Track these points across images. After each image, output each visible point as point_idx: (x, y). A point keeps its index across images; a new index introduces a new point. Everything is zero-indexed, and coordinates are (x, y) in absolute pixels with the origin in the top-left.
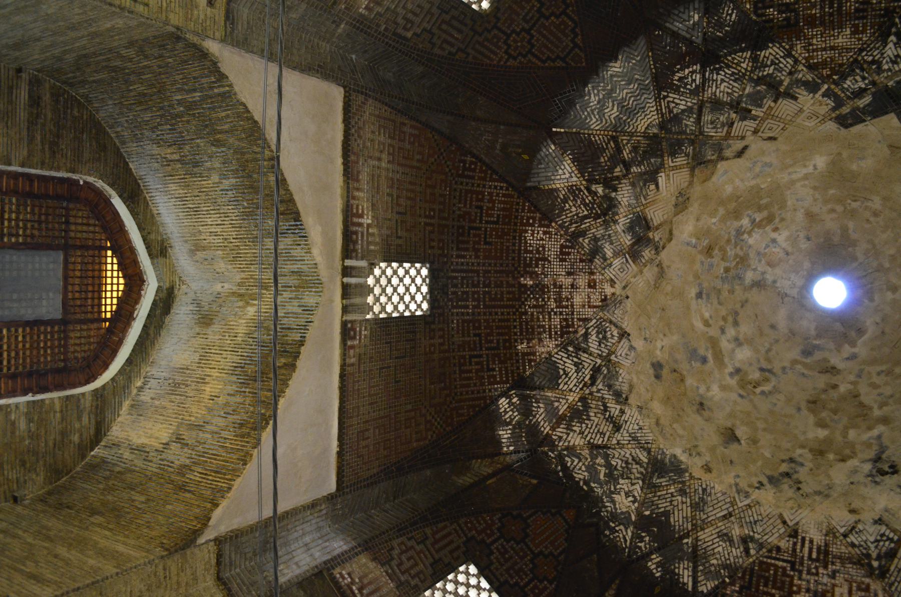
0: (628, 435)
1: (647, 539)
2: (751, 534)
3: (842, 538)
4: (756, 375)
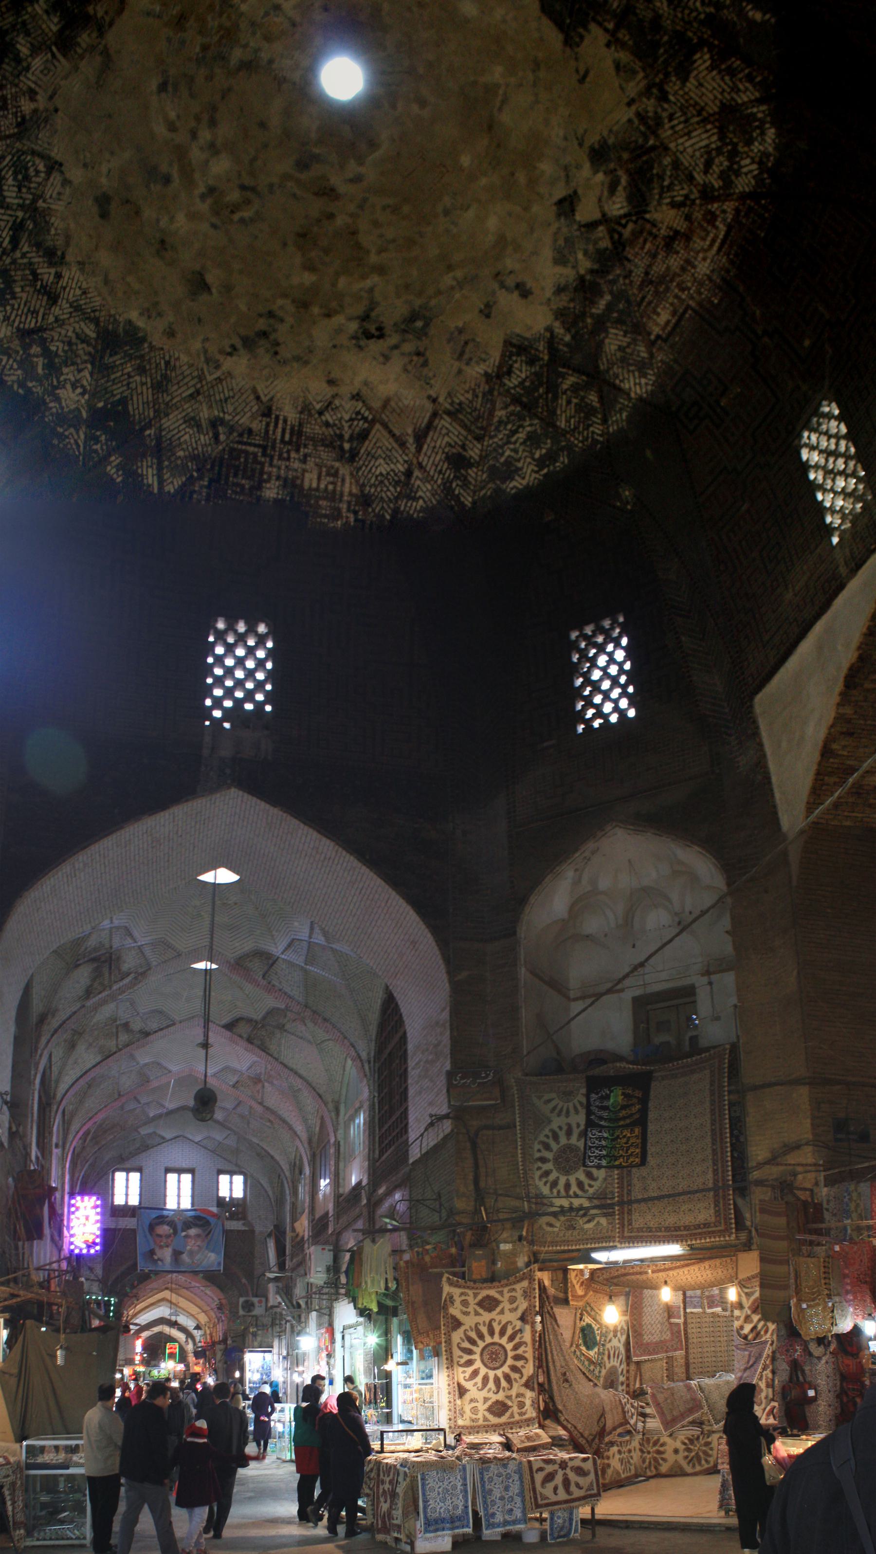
1: (103, 438)
2: (221, 415)
4: (235, 196)
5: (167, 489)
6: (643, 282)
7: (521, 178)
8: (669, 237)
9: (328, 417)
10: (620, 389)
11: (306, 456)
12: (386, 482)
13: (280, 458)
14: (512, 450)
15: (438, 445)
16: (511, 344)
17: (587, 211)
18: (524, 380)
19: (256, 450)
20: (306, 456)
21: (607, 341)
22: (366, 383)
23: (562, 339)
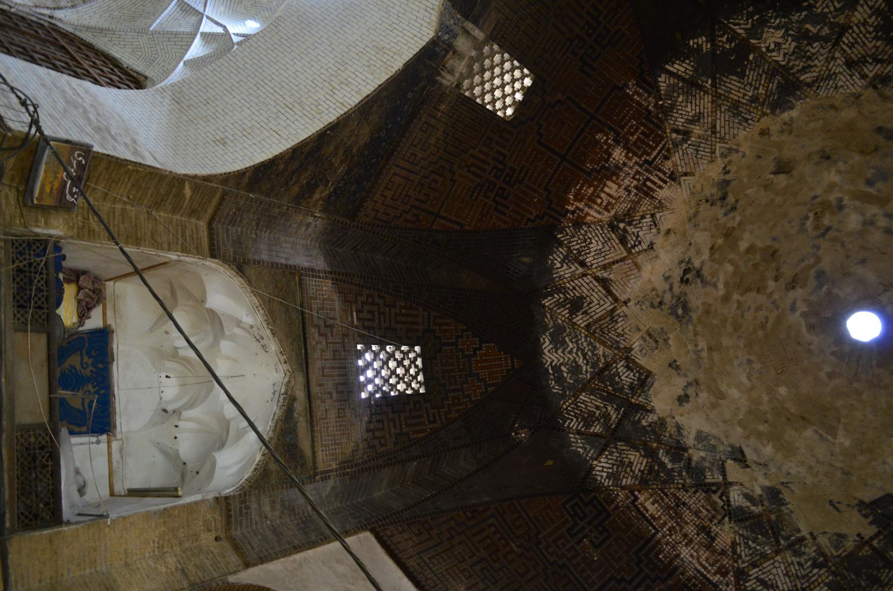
0: (837, 71)
2: (689, 142)
3: (652, 212)
4: (826, 221)
5: (663, 76)
6: (677, 498)
7: (763, 428)
8: (710, 532)
9: (648, 219)
10: (601, 453)
11: (630, 192)
12: (584, 244)
13: (638, 172)
14: (572, 349)
15: (594, 294)
16: (648, 376)
17: (733, 471)
18: (620, 378)
19: (652, 157)
20: (630, 192)
21: (638, 454)
22: (657, 256)
23: (644, 418)
